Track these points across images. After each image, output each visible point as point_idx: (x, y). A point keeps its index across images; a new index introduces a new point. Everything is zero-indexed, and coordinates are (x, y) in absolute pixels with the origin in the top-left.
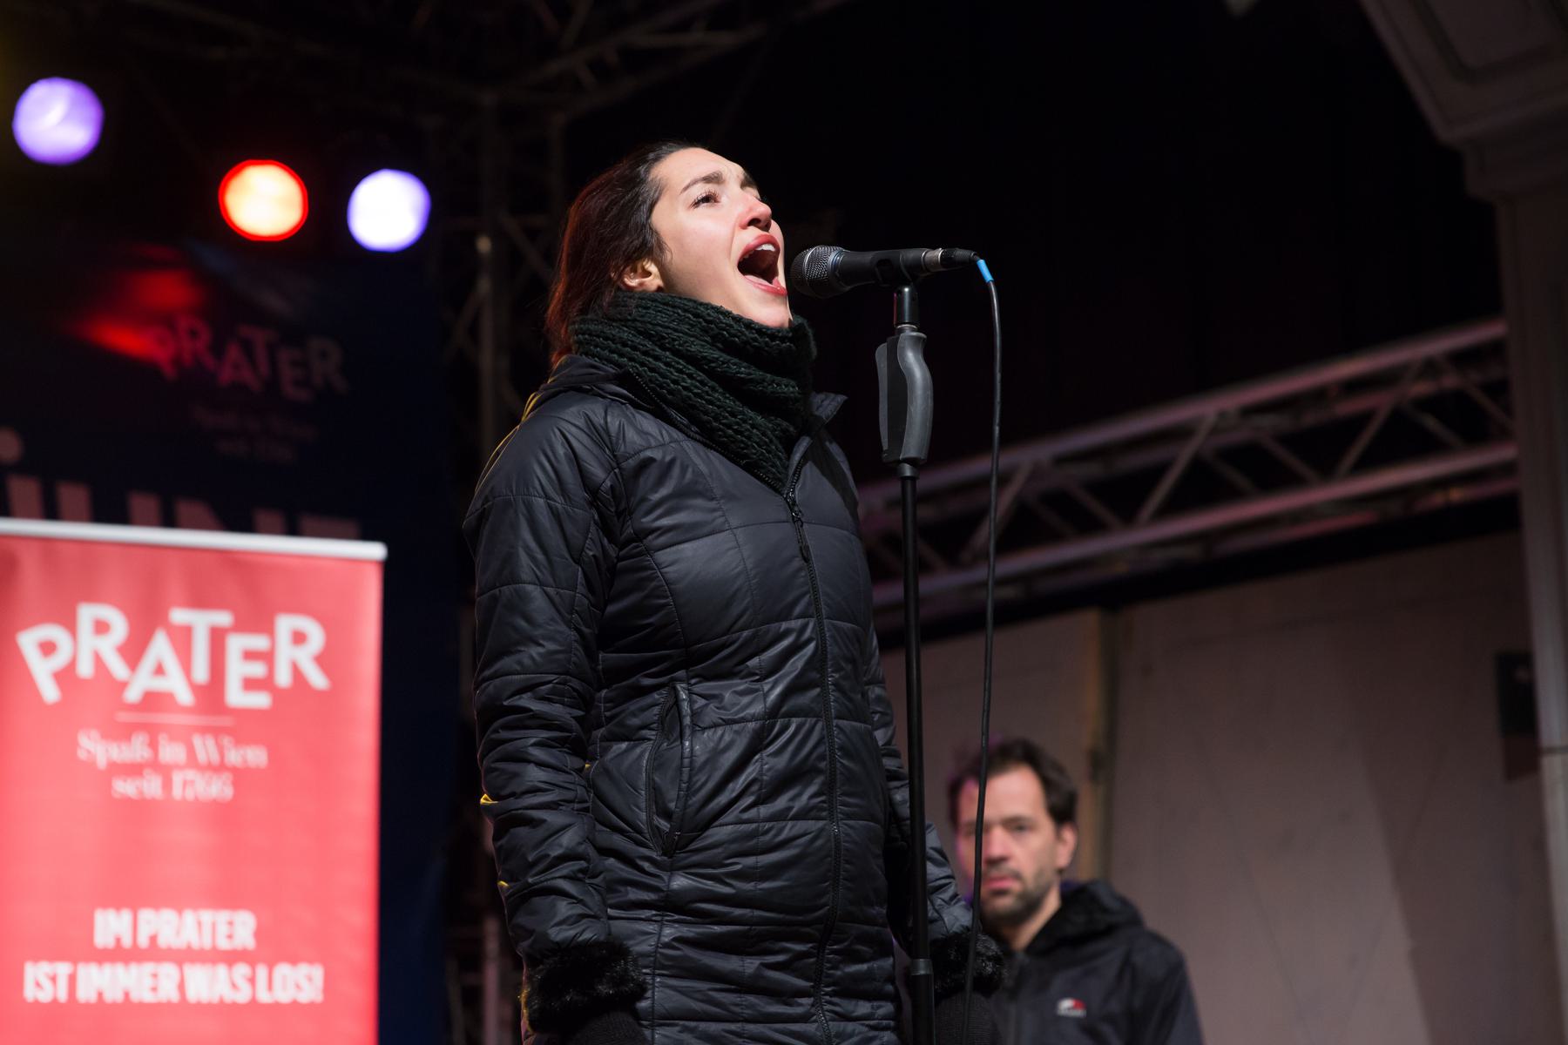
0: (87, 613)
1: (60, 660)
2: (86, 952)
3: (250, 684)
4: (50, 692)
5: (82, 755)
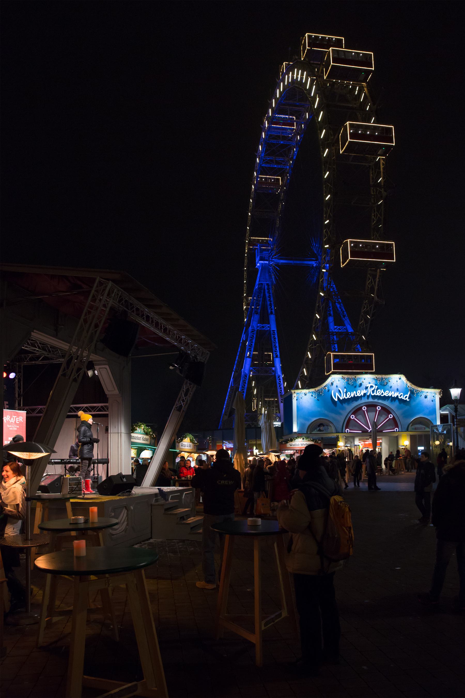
0: (8, 416)
1: (6, 419)
3: (18, 421)
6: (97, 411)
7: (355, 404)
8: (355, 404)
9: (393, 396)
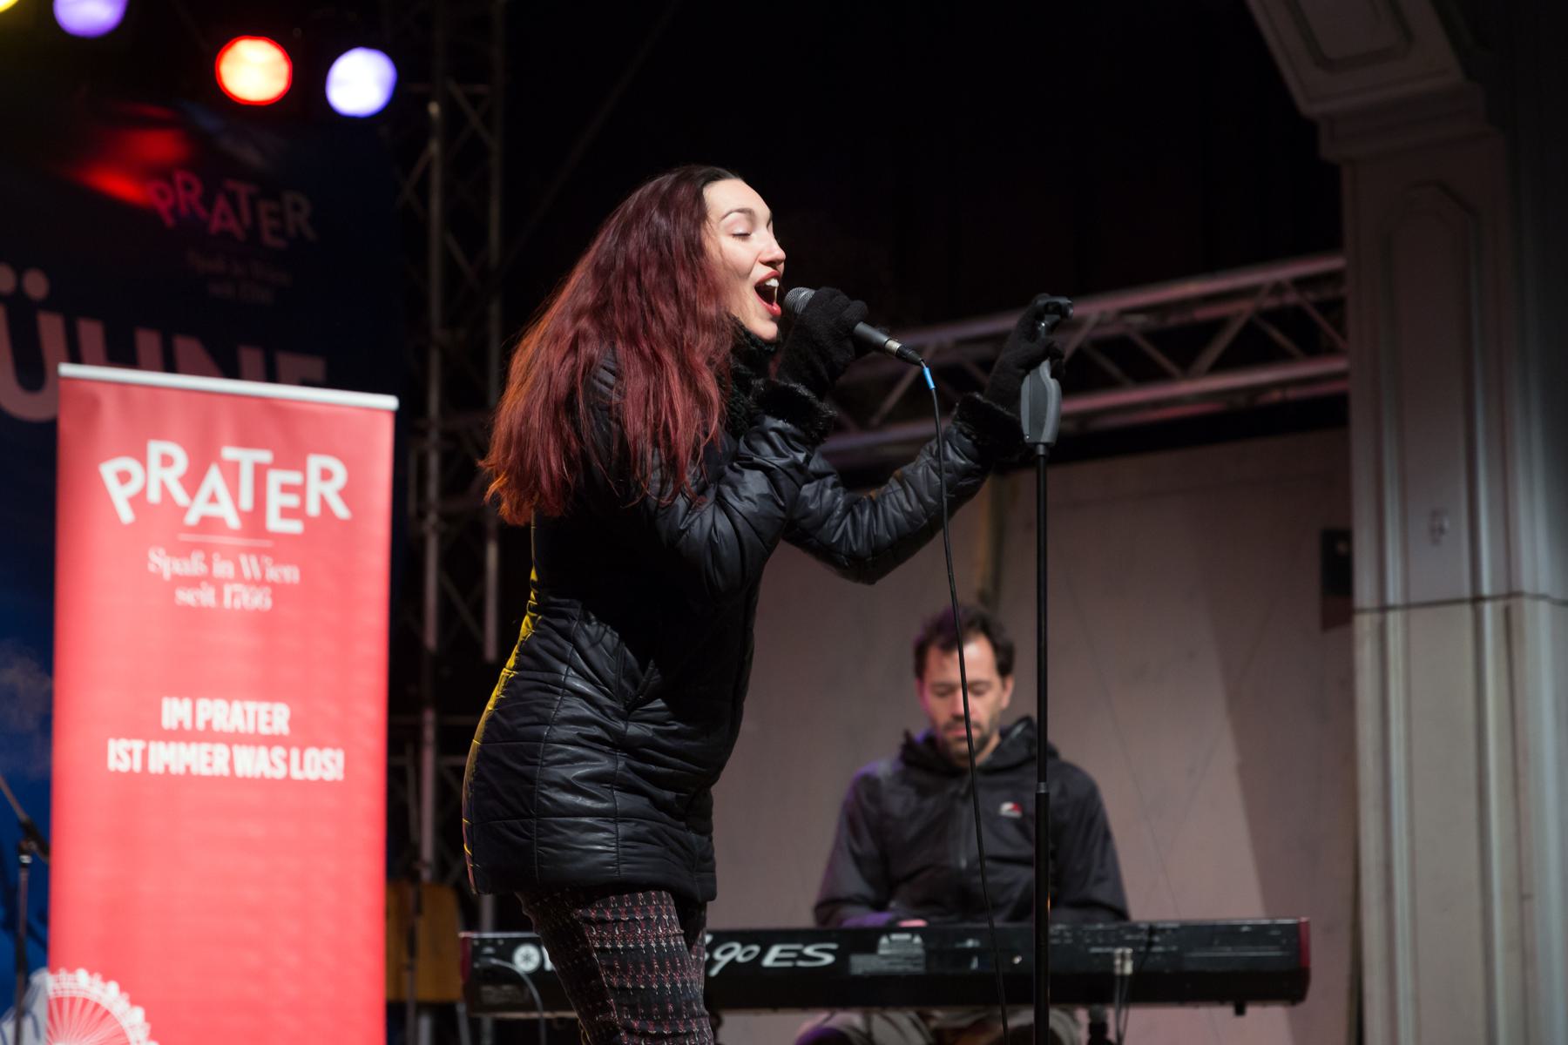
0: (156, 449)
1: (133, 487)
2: (153, 731)
3: (286, 513)
4: (126, 514)
5: (152, 568)
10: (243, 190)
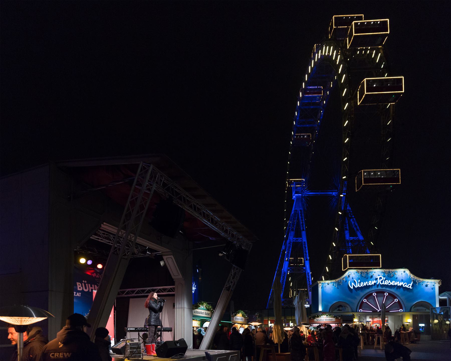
6: (167, 292)
7: (367, 291)
8: (367, 291)
9: (398, 285)
10: (99, 274)
